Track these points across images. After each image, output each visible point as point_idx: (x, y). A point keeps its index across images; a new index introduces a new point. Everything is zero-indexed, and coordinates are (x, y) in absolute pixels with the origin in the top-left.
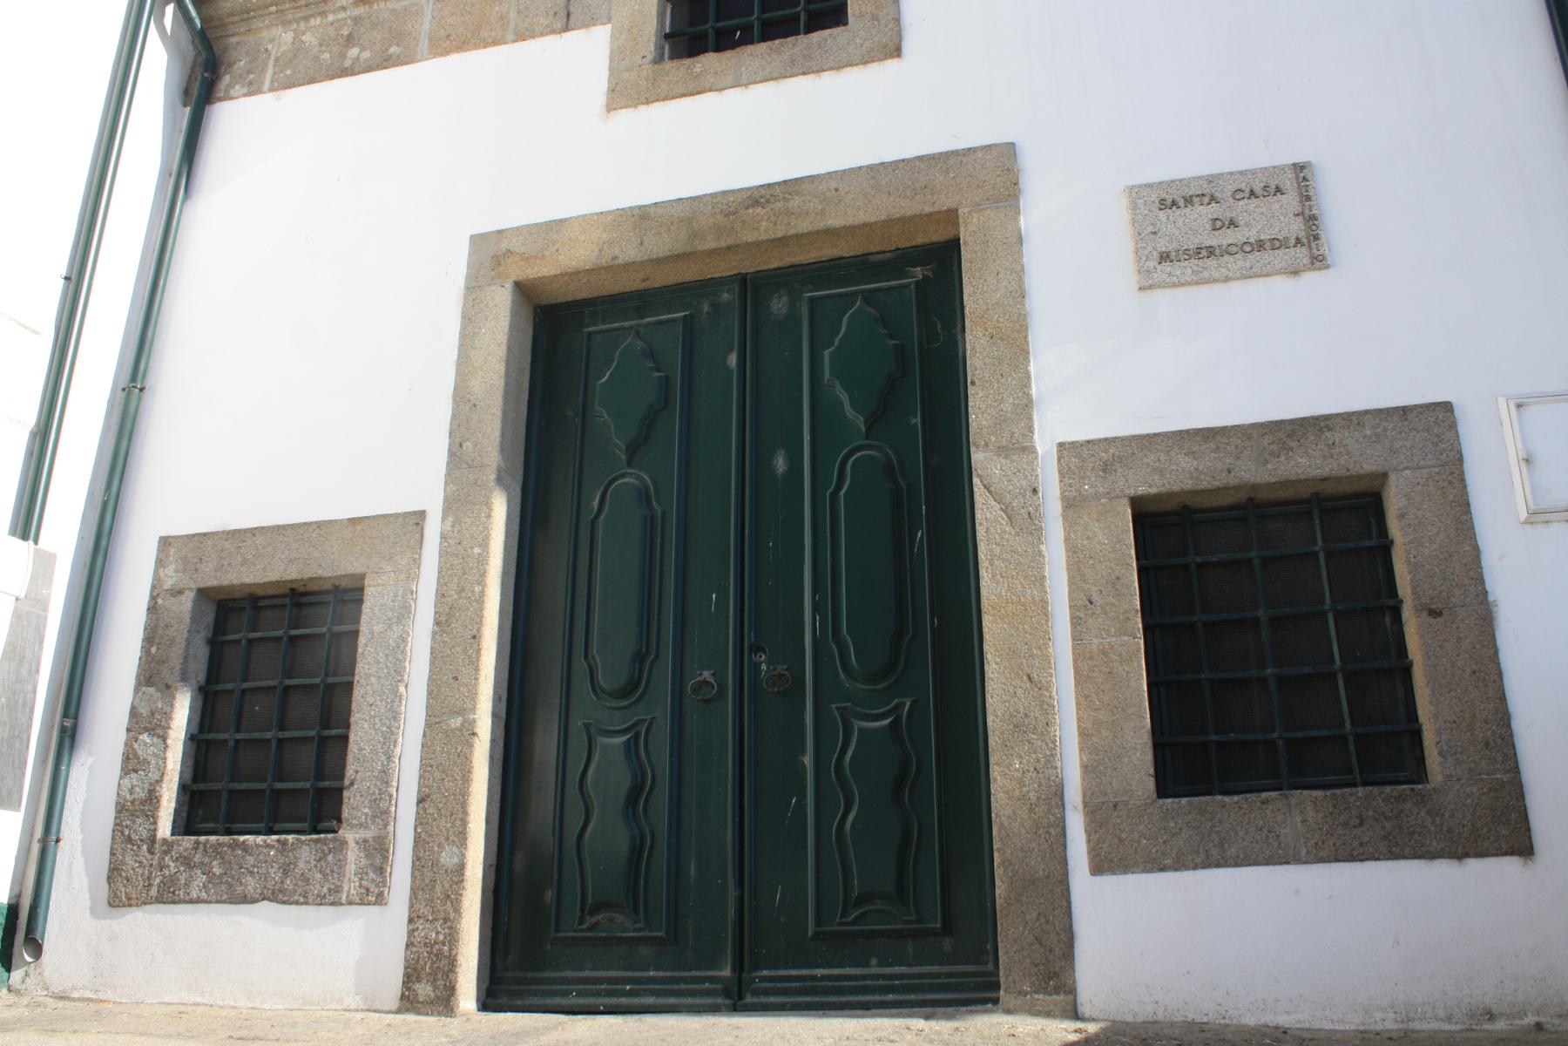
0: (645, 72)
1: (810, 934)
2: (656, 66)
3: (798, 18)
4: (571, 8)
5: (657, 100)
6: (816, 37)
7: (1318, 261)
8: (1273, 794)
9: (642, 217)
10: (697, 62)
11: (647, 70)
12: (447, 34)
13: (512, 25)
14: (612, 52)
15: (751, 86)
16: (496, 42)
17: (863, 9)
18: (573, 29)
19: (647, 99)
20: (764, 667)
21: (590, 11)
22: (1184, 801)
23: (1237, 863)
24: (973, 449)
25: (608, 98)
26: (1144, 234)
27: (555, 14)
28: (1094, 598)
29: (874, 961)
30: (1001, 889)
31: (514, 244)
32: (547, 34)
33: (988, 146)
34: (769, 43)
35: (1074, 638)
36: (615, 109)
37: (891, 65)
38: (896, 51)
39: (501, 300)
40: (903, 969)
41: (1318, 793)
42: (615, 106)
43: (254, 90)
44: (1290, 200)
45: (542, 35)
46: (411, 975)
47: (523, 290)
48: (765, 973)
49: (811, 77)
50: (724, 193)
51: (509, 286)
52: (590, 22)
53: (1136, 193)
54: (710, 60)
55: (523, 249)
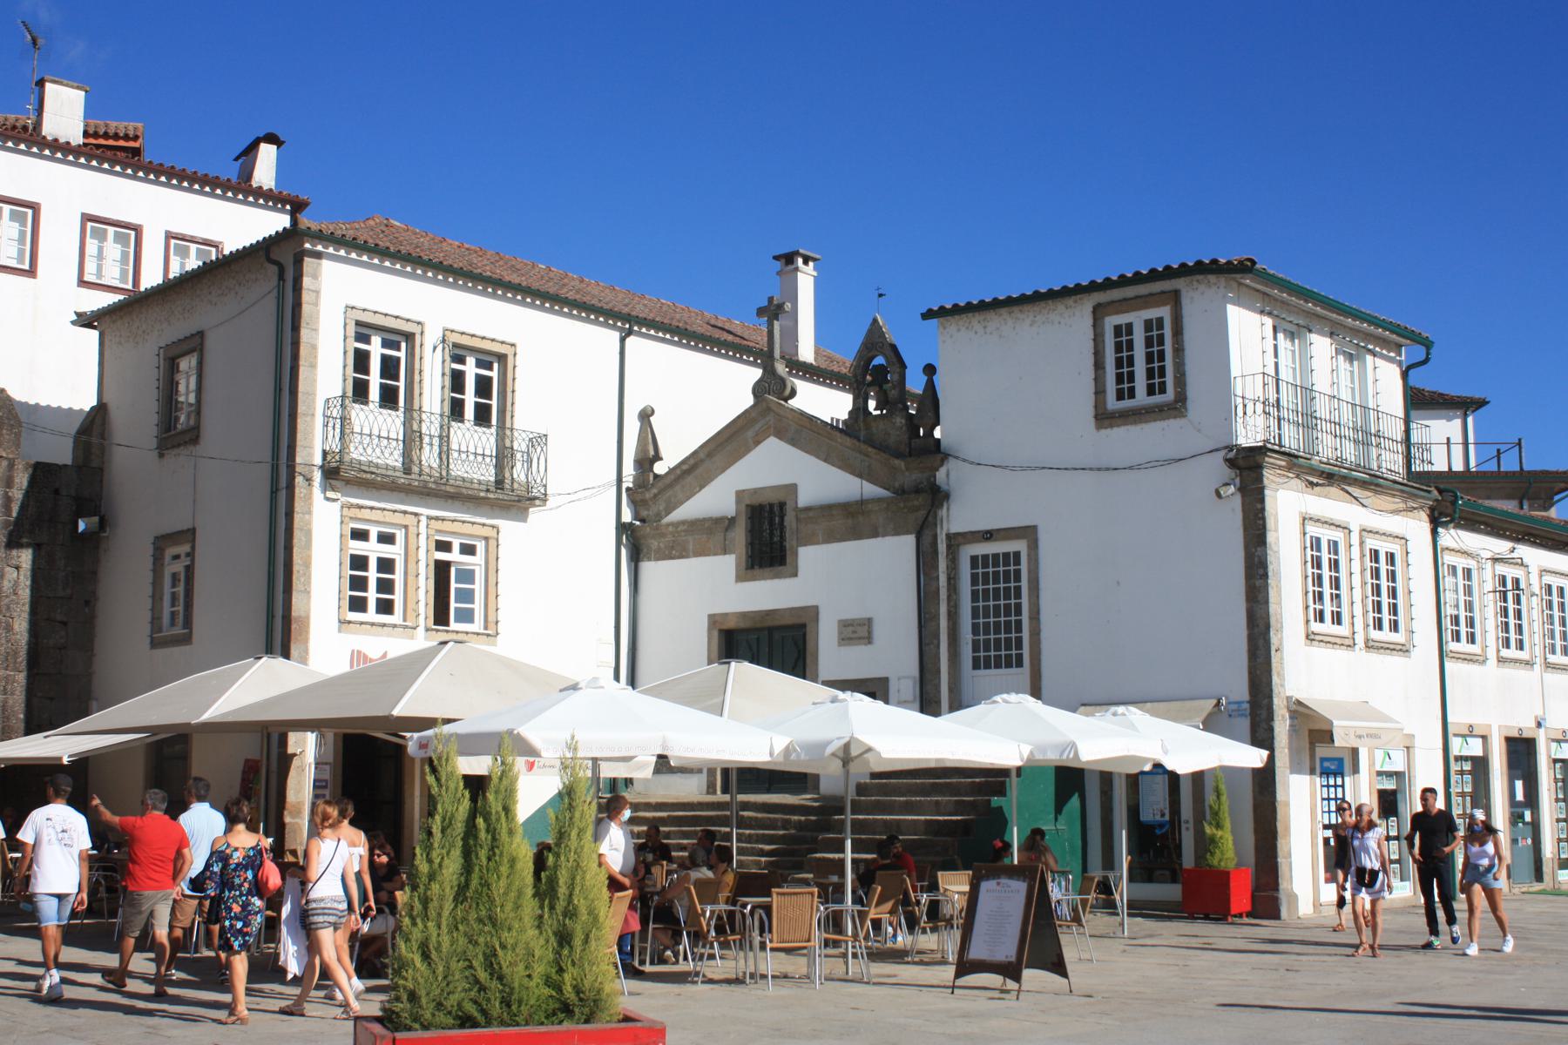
7: (870, 643)
9: (744, 615)
26: (840, 633)
38: (796, 575)
39: (716, 633)
43: (649, 560)
44: (866, 627)
46: (708, 787)
47: (721, 631)
52: (730, 553)
53: (840, 621)
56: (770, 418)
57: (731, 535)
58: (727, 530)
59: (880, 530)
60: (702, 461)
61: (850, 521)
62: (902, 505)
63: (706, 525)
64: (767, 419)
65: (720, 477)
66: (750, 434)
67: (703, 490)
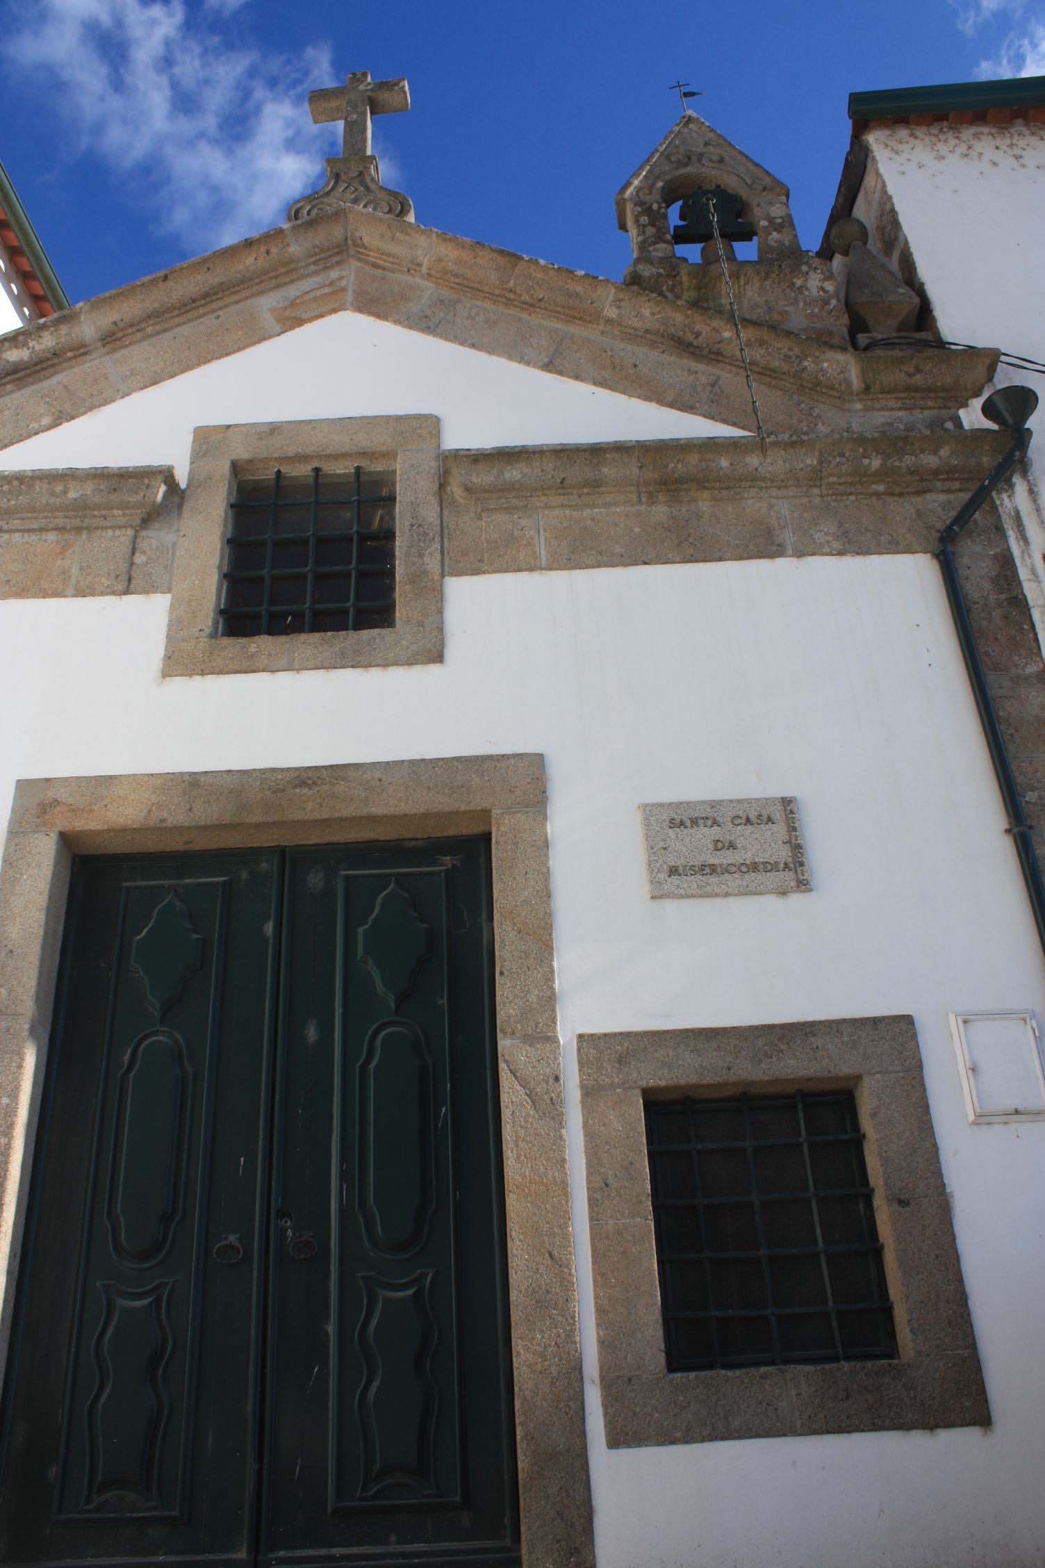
0: (201, 644)
1: (329, 1510)
2: (213, 640)
3: (348, 612)
4: (133, 573)
5: (212, 673)
6: (365, 634)
7: (803, 885)
8: (770, 1369)
9: (192, 783)
10: (253, 642)
11: (204, 642)
12: (6, 579)
13: (73, 581)
14: (170, 621)
15: (303, 671)
16: (55, 594)
17: (410, 614)
18: (133, 594)
19: (202, 670)
20: (290, 1233)
21: (151, 578)
22: (692, 1375)
23: (741, 1436)
24: (499, 1036)
25: (163, 665)
26: (656, 849)
27: (117, 576)
28: (611, 1180)
29: (393, 1538)
30: (523, 1463)
31: (63, 795)
32: (107, 594)
33: (520, 754)
34: (322, 634)
35: (591, 1219)
36: (170, 676)
37: (434, 669)
38: (437, 656)
39: (45, 849)
40: (421, 1547)
41: (810, 1368)
42: (171, 673)
44: (779, 829)
45: (102, 594)
47: (67, 841)
48: (282, 1553)
49: (359, 670)
50: (273, 770)
51: (54, 835)
53: (650, 811)
54: (263, 644)
55: (71, 801)
56: (348, 274)
57: (157, 537)
58: (146, 522)
59: (788, 537)
60: (80, 351)
61: (660, 512)
62: (876, 463)
63: (72, 495)
64: (334, 274)
65: (137, 397)
66: (267, 304)
67: (66, 427)
